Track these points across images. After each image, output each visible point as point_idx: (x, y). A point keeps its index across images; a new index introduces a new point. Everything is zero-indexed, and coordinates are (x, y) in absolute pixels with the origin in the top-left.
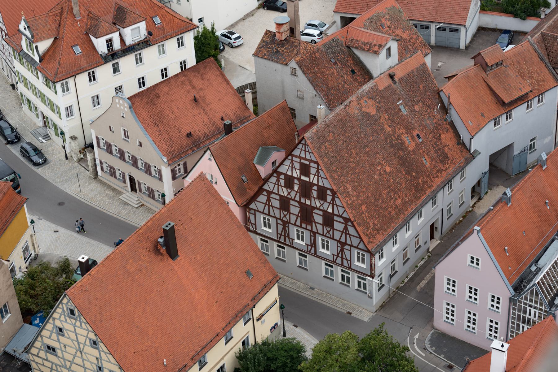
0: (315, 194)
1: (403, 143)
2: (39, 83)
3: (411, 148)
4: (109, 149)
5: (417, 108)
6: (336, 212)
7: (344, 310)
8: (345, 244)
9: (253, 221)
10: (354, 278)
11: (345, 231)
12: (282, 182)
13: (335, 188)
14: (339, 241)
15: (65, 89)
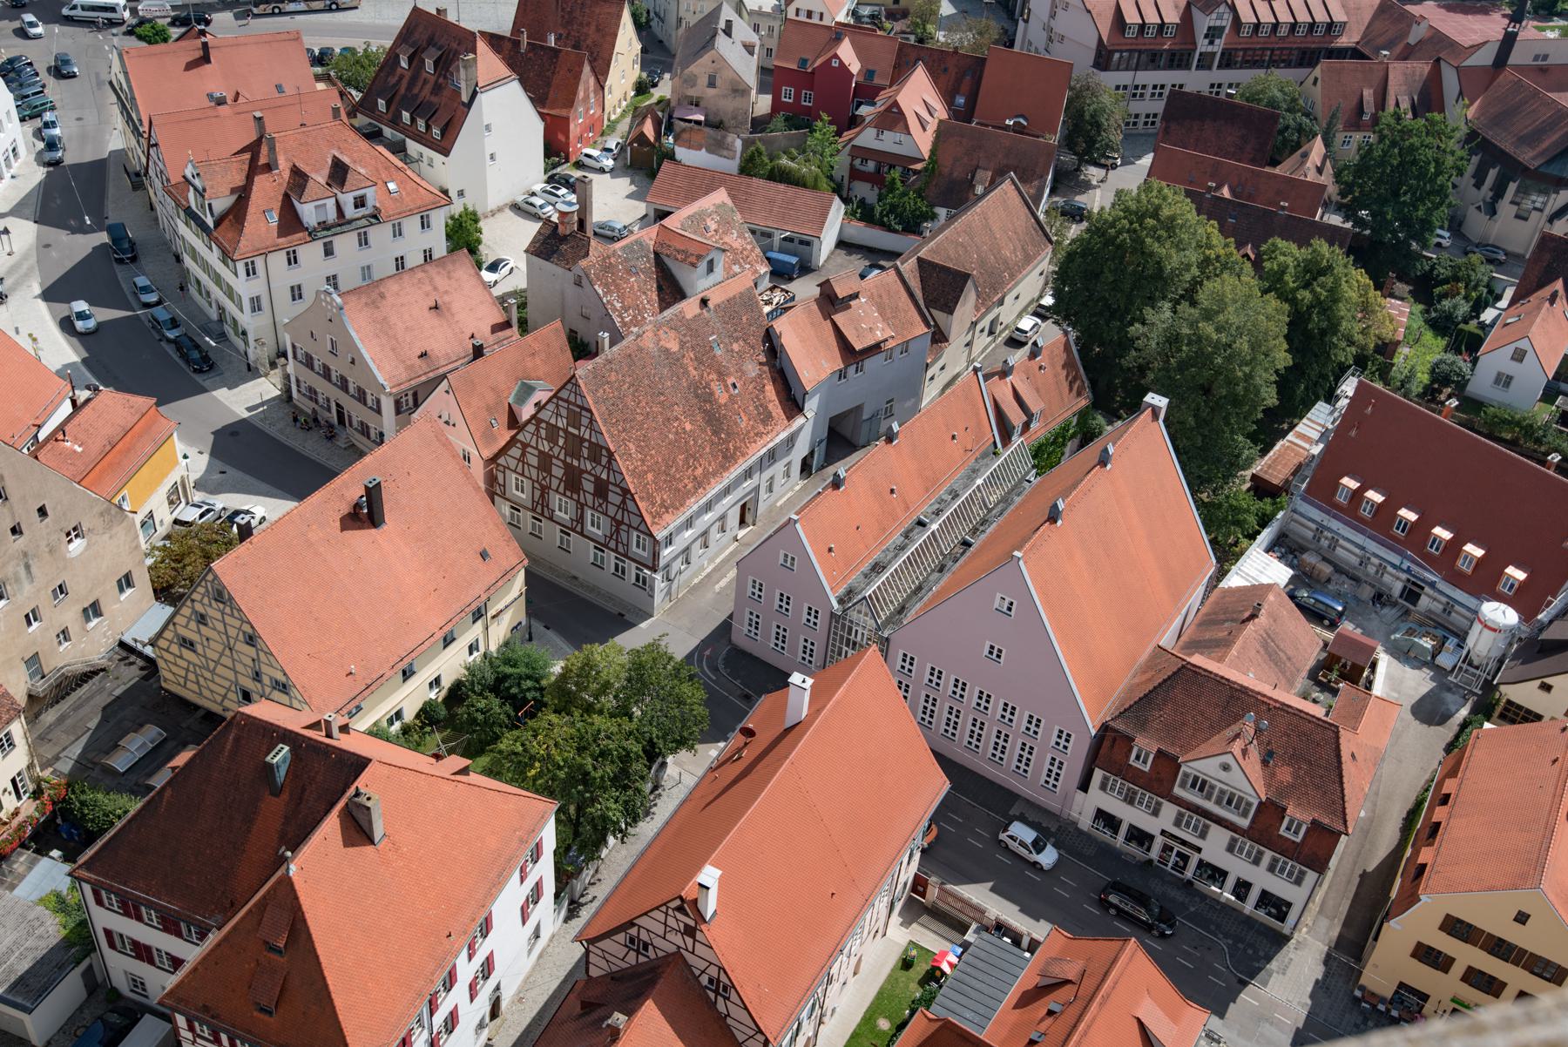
0: (585, 452)
1: (712, 394)
2: (213, 257)
3: (722, 401)
4: (309, 362)
5: (736, 347)
6: (612, 480)
7: (615, 610)
8: (622, 522)
9: (501, 480)
10: (632, 568)
11: (622, 507)
12: (543, 433)
13: (612, 448)
14: (613, 519)
15: (251, 271)
